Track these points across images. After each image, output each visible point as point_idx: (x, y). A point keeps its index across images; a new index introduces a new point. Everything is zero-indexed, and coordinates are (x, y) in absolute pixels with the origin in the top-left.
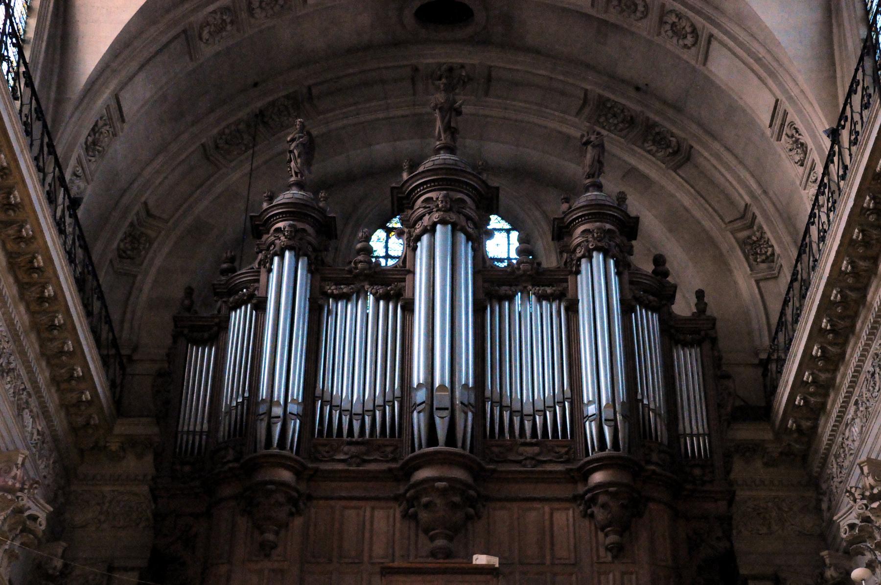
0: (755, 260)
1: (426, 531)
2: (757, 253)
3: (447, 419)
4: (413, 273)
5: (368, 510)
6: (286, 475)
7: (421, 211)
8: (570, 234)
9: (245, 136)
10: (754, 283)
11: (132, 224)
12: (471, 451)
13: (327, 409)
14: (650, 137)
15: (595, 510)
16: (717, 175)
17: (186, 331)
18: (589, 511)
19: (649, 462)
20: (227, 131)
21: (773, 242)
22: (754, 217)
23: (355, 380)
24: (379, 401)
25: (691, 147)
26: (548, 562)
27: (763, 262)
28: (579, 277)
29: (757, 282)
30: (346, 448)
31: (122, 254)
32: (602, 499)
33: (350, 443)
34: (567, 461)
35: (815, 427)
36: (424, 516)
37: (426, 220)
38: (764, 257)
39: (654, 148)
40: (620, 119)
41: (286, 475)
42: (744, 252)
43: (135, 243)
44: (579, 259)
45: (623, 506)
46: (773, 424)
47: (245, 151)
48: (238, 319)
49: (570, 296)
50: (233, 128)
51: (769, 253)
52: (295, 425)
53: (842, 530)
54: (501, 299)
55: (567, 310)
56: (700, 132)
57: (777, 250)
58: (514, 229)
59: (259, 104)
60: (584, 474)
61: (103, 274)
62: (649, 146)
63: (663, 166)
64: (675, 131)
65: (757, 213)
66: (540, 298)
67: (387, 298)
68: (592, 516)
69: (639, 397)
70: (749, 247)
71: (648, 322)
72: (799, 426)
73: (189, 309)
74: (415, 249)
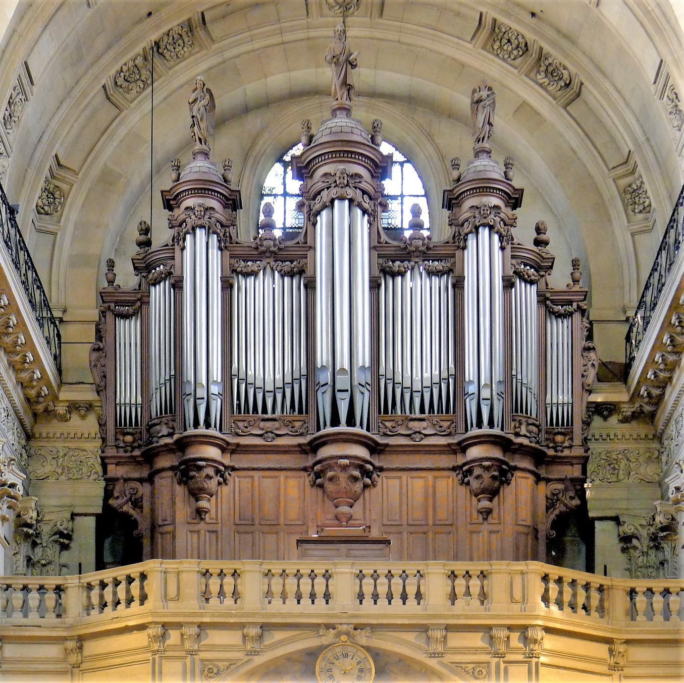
0: (634, 211)
1: (333, 499)
2: (635, 203)
3: (347, 400)
4: (313, 248)
5: (282, 479)
6: (212, 452)
7: (320, 185)
8: (459, 205)
9: (143, 72)
10: (630, 236)
11: (47, 180)
12: (368, 430)
13: (243, 387)
14: (543, 68)
15: (470, 478)
16: (605, 115)
17: (112, 305)
18: (466, 480)
19: (517, 435)
20: (125, 68)
21: (650, 194)
22: (635, 166)
23: (268, 364)
24: (288, 379)
25: (582, 84)
26: (430, 523)
27: (640, 212)
28: (466, 252)
29: (633, 235)
30: (262, 424)
31: (40, 210)
32: (477, 471)
33: (264, 420)
34: (449, 435)
35: (662, 395)
36: (329, 487)
37: (325, 196)
38: (641, 208)
39: (546, 81)
40: (514, 46)
41: (212, 452)
42: (623, 202)
43: (52, 199)
44: (467, 234)
45: (494, 478)
46: (628, 391)
47: (144, 89)
48: (159, 295)
49: (457, 272)
50: (131, 64)
51: (646, 204)
52: (216, 406)
53: (670, 492)
54: (394, 275)
55: (454, 286)
56: (590, 68)
57: (653, 205)
58: (408, 161)
59: (154, 37)
60: (462, 447)
61: (28, 235)
62: (541, 78)
63: (554, 102)
64: (567, 63)
65: (639, 163)
66: (430, 273)
67: (291, 275)
68: (468, 483)
69: (514, 373)
70: (629, 196)
71: (526, 295)
72: (649, 394)
73: (111, 282)
74: (314, 224)
